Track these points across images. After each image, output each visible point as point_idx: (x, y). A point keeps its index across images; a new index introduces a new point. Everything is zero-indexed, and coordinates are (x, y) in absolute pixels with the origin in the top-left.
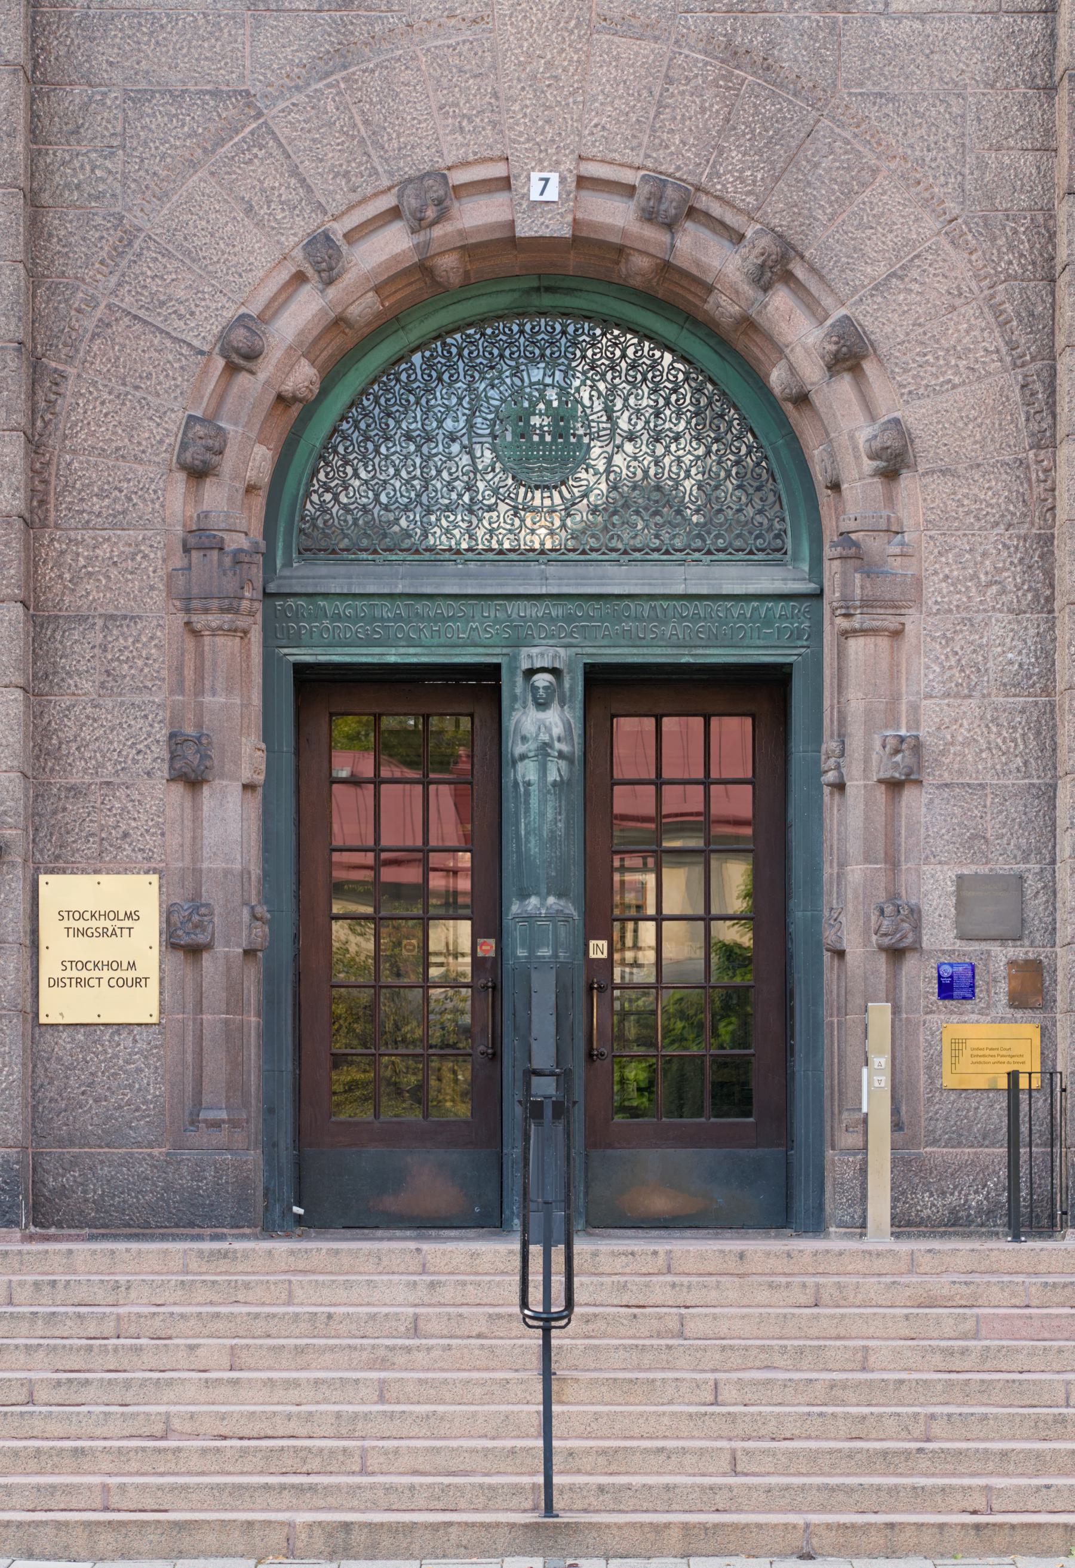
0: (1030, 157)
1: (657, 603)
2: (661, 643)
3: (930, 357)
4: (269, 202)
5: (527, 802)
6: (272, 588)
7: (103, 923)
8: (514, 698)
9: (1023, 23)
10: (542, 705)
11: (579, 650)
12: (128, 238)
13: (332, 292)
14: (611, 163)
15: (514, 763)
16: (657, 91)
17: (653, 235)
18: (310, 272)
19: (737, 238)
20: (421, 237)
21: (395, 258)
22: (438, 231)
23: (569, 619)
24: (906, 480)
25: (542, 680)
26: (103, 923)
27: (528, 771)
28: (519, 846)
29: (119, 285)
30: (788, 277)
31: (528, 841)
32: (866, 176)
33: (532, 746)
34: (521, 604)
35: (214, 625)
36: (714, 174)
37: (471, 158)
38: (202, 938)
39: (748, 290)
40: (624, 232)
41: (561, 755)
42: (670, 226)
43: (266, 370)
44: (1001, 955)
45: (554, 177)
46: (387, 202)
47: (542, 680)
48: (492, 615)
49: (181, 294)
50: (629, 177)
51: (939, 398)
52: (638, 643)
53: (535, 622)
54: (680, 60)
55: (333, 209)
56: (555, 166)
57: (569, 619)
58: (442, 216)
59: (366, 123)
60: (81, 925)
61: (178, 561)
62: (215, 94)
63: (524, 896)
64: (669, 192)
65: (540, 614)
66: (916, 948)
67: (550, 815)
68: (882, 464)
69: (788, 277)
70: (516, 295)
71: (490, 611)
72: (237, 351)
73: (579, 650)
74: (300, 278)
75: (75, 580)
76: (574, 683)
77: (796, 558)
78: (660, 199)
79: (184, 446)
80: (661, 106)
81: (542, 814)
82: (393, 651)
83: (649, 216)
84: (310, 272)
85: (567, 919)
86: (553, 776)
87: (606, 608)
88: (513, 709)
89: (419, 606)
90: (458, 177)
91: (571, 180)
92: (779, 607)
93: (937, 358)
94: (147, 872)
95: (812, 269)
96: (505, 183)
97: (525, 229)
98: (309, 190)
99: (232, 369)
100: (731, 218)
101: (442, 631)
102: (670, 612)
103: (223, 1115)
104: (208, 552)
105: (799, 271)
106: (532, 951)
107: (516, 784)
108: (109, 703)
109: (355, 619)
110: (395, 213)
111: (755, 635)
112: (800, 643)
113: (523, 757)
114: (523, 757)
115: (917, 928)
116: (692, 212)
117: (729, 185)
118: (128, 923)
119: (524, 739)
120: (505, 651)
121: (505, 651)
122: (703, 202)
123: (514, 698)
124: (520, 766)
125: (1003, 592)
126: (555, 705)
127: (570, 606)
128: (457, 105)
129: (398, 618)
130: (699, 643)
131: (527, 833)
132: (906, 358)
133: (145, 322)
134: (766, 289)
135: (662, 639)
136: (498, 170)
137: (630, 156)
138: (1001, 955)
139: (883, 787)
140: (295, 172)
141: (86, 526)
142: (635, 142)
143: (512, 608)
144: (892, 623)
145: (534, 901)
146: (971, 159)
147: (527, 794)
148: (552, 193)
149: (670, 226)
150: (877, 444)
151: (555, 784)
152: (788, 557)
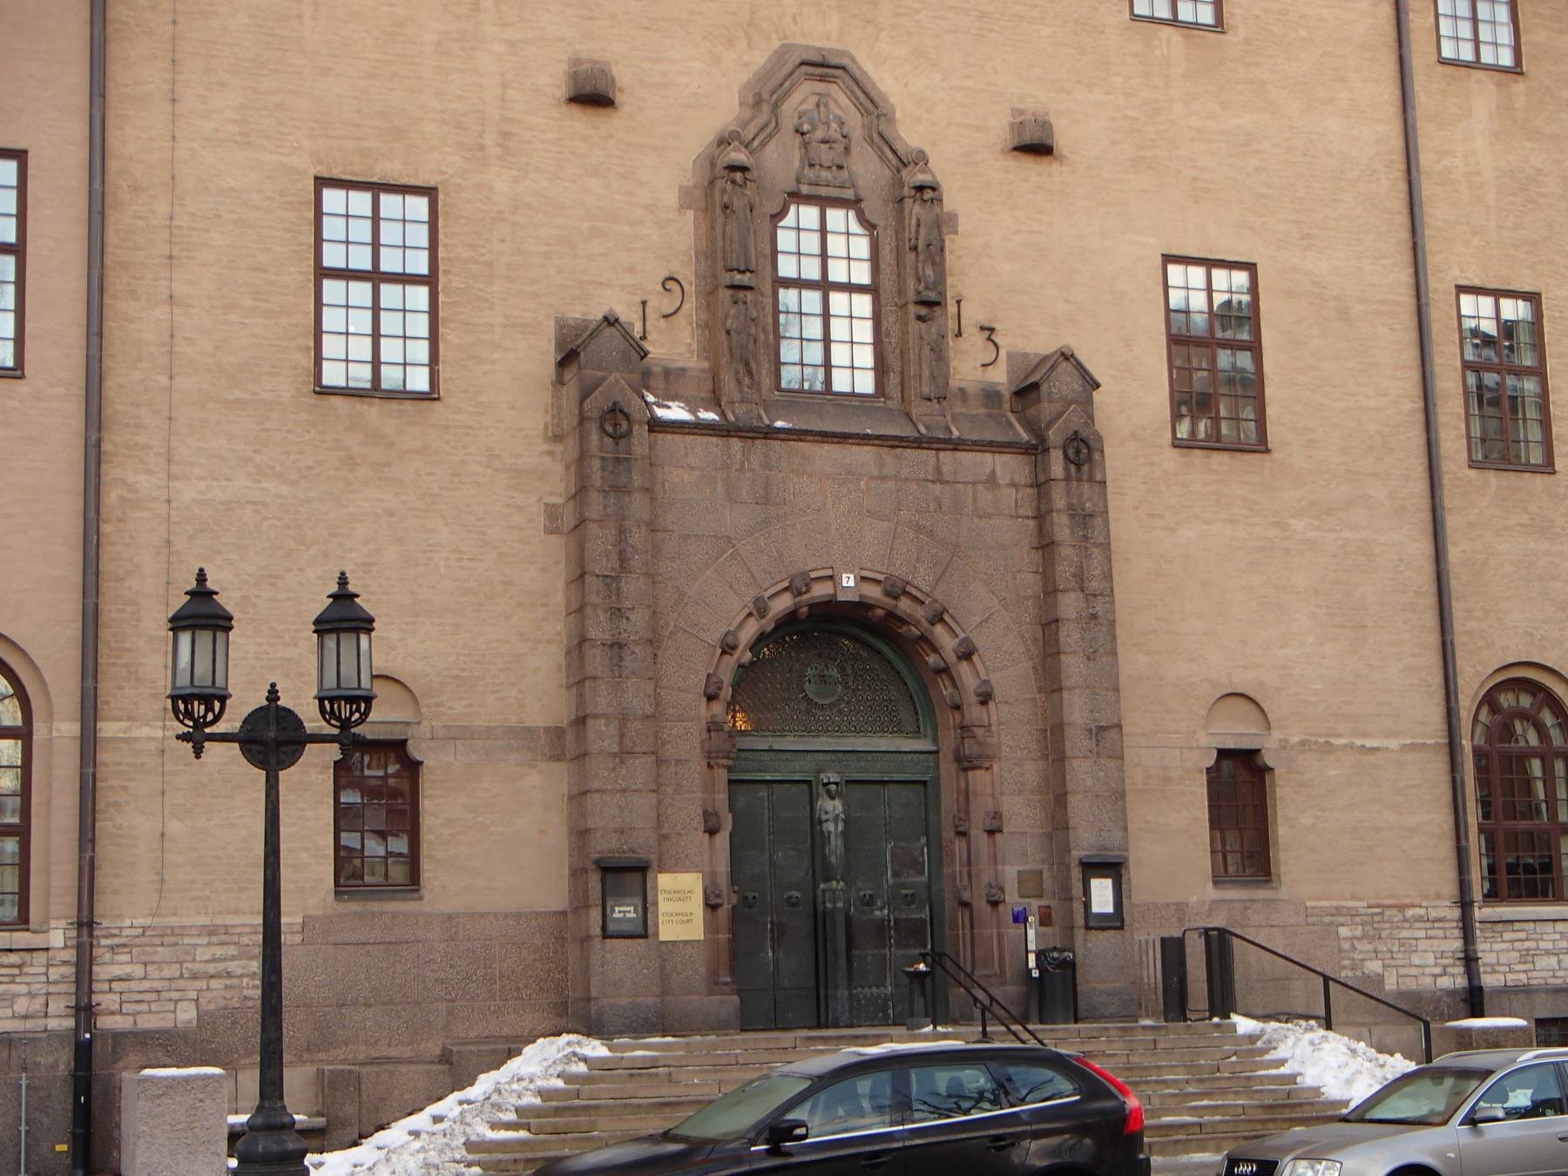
0: (1032, 575)
7: (678, 895)
9: (1026, 521)
10: (832, 798)
12: (682, 595)
13: (763, 621)
14: (874, 571)
17: (889, 602)
20: (797, 600)
22: (804, 597)
24: (992, 705)
26: (678, 895)
29: (679, 616)
30: (942, 620)
31: (829, 856)
36: (914, 577)
38: (719, 901)
39: (926, 624)
40: (876, 600)
42: (896, 598)
43: (737, 654)
44: (1035, 904)
45: (852, 576)
46: (786, 584)
47: (833, 787)
49: (703, 621)
50: (880, 577)
54: (899, 530)
55: (765, 586)
56: (851, 572)
59: (777, 551)
60: (670, 896)
61: (705, 735)
62: (715, 536)
66: (1004, 901)
67: (839, 843)
68: (980, 698)
69: (942, 620)
71: (808, 757)
72: (728, 646)
74: (750, 615)
75: (663, 744)
80: (892, 548)
81: (836, 846)
83: (888, 594)
84: (755, 612)
87: (854, 756)
90: (813, 575)
91: (859, 578)
92: (922, 757)
94: (696, 872)
95: (952, 617)
97: (841, 598)
98: (755, 579)
99: (724, 652)
100: (918, 595)
103: (729, 980)
105: (947, 618)
106: (834, 903)
108: (678, 797)
109: (753, 761)
110: (786, 589)
113: (826, 821)
114: (826, 821)
115: (1004, 892)
116: (906, 593)
117: (919, 582)
118: (689, 895)
122: (909, 589)
125: (1029, 752)
127: (840, 755)
133: (690, 633)
134: (933, 625)
137: (881, 569)
138: (1035, 904)
140: (749, 570)
141: (667, 720)
143: (816, 755)
144: (987, 764)
145: (834, 883)
146: (1010, 575)
147: (829, 836)
148: (851, 583)
149: (896, 598)
150: (980, 690)
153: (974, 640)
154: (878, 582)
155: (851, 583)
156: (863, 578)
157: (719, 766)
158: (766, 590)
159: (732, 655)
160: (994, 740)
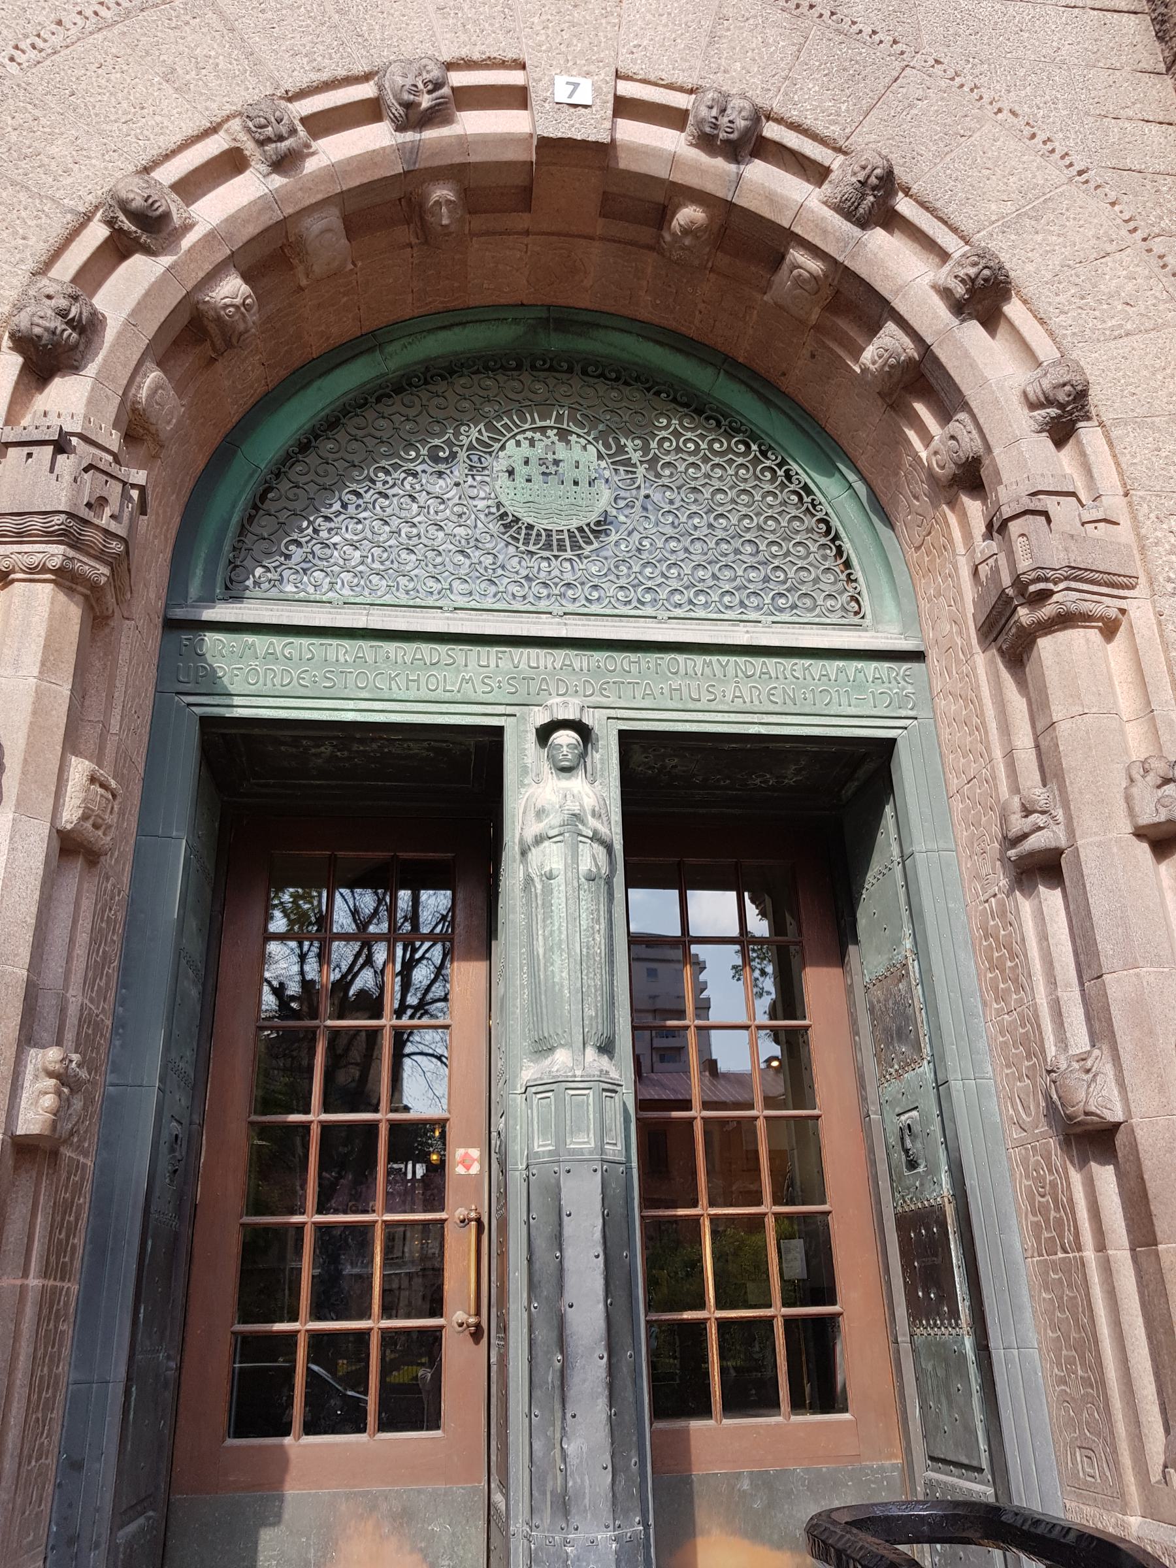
1: (714, 658)
2: (720, 708)
3: (1089, 299)
4: (199, 69)
5: (547, 905)
6: (179, 613)
8: (525, 770)
11: (612, 713)
15: (524, 853)
16: (707, 24)
18: (249, 147)
19: (817, 173)
20: (409, 136)
21: (371, 159)
22: (430, 134)
23: (597, 672)
24: (1088, 434)
25: (565, 738)
27: (551, 857)
28: (533, 973)
30: (890, 220)
31: (549, 962)
32: (974, 125)
33: (553, 821)
34: (534, 652)
35: (36, 560)
37: (476, 56)
40: (674, 160)
41: (596, 838)
48: (493, 665)
51: (1112, 344)
52: (691, 706)
53: (552, 675)
57: (597, 672)
58: (436, 116)
63: (543, 1048)
64: (736, 102)
65: (558, 666)
68: (1053, 411)
70: (519, 330)
72: (124, 205)
73: (612, 713)
76: (607, 755)
77: (877, 620)
78: (723, 111)
79: (19, 308)
80: (713, 38)
81: (573, 919)
82: (351, 705)
83: (707, 141)
84: (249, 147)
85: (612, 1089)
86: (586, 865)
88: (522, 784)
89: (391, 648)
90: (458, 79)
93: (1100, 302)
96: (518, 98)
101: (423, 680)
102: (731, 669)
104: (35, 450)
105: (904, 206)
106: (560, 1141)
107: (529, 880)
111: (844, 700)
112: (903, 713)
113: (539, 840)
114: (539, 840)
119: (540, 813)
120: (510, 710)
121: (510, 710)
122: (772, 131)
123: (525, 770)
124: (534, 855)
126: (580, 772)
128: (461, 8)
129: (360, 660)
130: (772, 708)
131: (549, 950)
132: (1061, 298)
135: (722, 702)
136: (514, 78)
137: (680, 78)
139: (1145, 846)
142: (686, 65)
144: (1108, 606)
147: (548, 891)
151: (591, 879)
152: (868, 621)
153: (1004, 257)
154: (674, 118)
155: (584, 96)
156: (624, 107)
157: (35, 572)
158: (291, 98)
159: (148, 251)
160: (1124, 533)
